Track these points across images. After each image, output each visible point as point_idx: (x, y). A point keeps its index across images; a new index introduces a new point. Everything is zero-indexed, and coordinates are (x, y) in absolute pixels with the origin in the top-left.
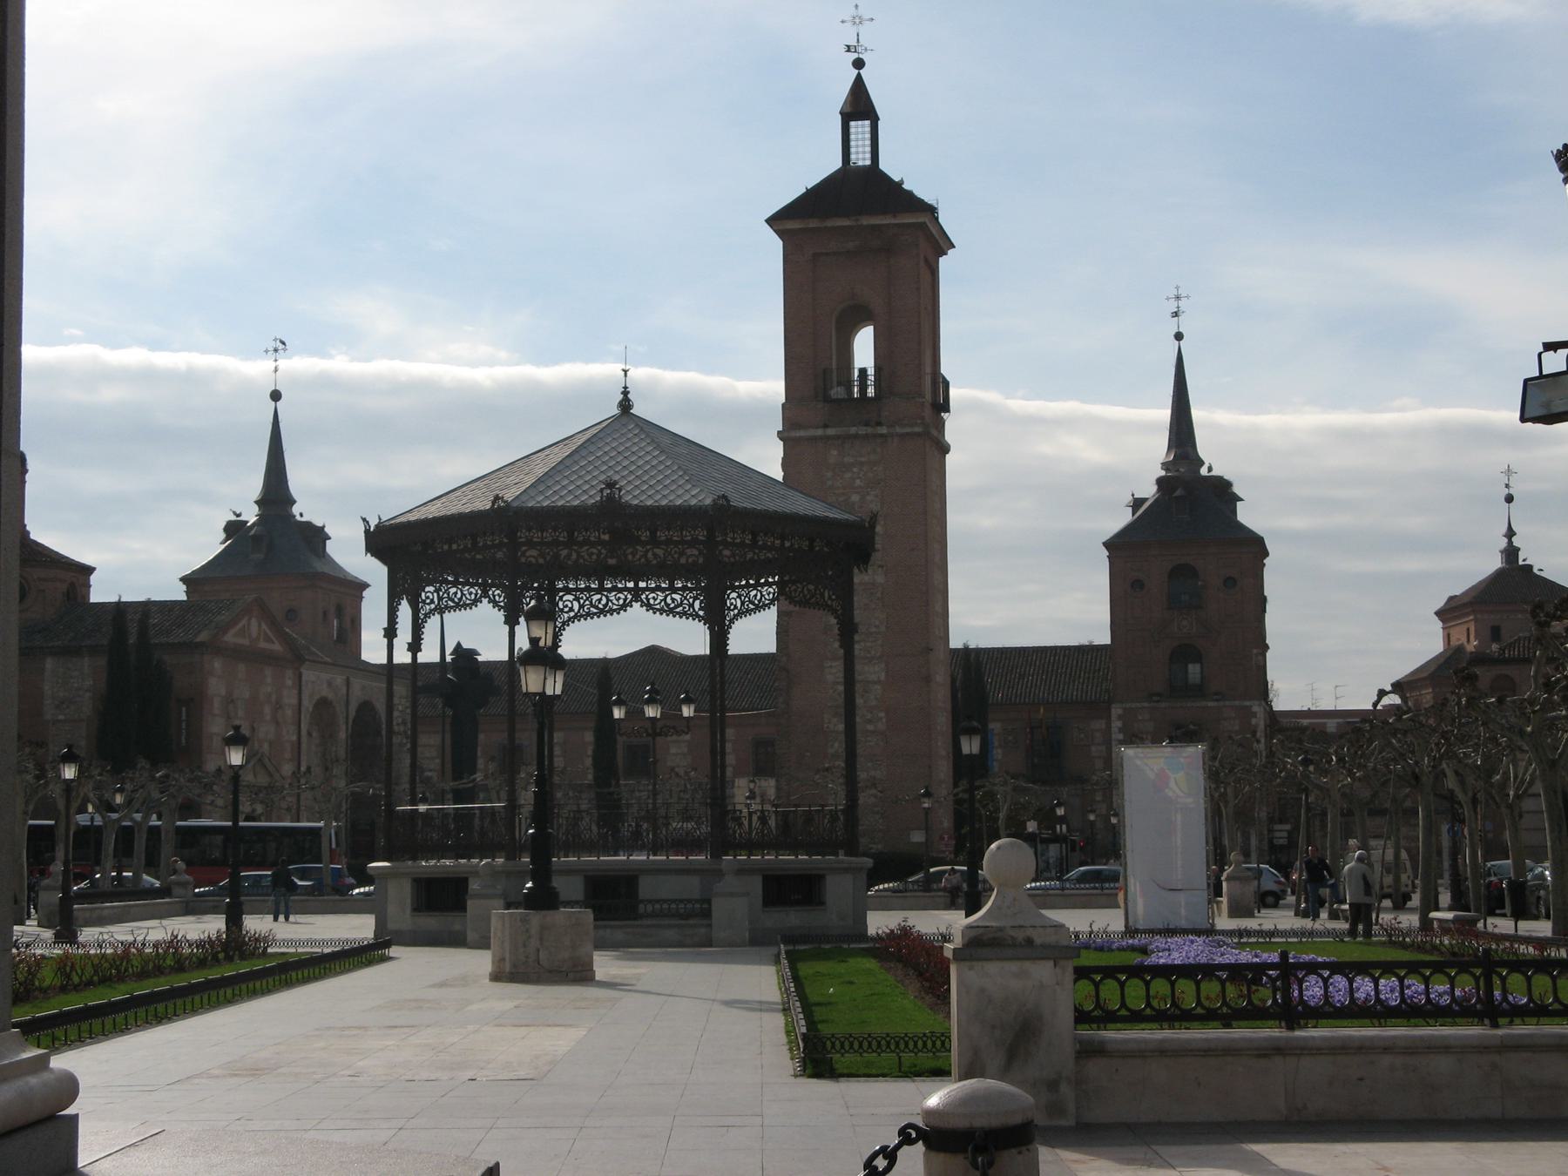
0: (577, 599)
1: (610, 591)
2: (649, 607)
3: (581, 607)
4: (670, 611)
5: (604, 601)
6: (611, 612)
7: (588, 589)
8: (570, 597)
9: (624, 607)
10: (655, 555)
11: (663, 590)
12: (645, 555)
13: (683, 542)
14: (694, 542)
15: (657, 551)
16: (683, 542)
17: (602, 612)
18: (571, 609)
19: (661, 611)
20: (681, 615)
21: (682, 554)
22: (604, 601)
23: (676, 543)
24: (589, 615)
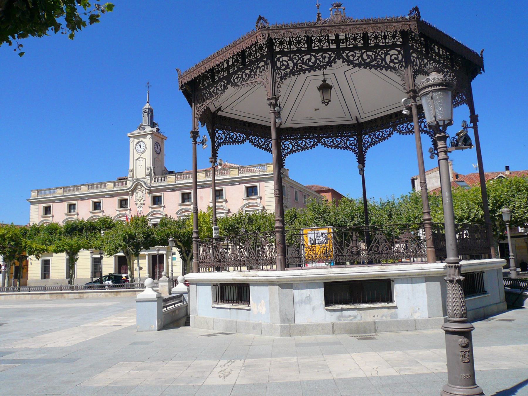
0: (291, 143)
1: (306, 138)
2: (326, 145)
3: (293, 146)
4: (335, 147)
5: (304, 143)
6: (308, 148)
7: (297, 139)
8: (288, 142)
9: (313, 146)
10: (368, 56)
11: (332, 137)
12: (362, 56)
13: (386, 46)
14: (394, 46)
15: (370, 53)
16: (386, 46)
17: (303, 149)
18: (289, 148)
19: (332, 147)
20: (342, 148)
21: (386, 54)
22: (304, 143)
23: (382, 48)
24: (298, 150)
